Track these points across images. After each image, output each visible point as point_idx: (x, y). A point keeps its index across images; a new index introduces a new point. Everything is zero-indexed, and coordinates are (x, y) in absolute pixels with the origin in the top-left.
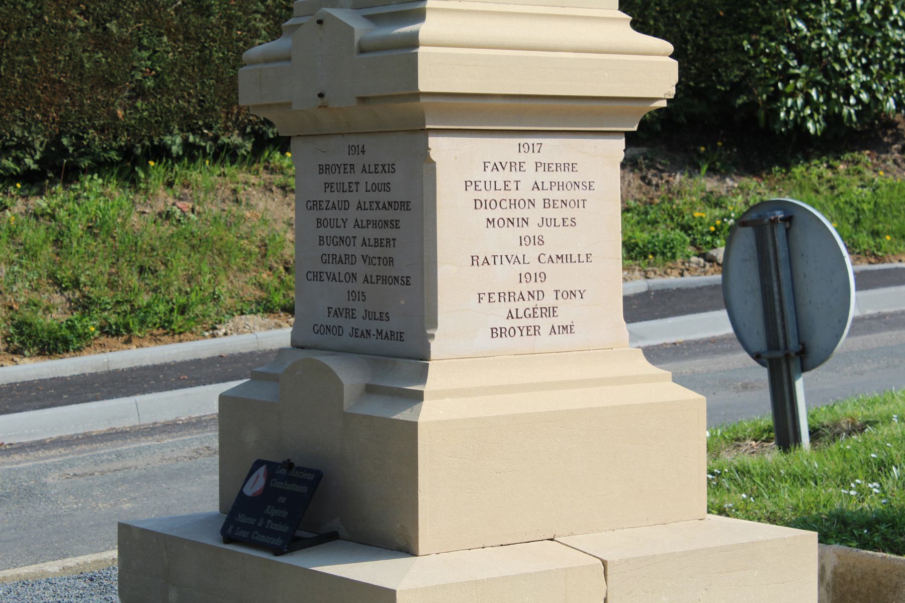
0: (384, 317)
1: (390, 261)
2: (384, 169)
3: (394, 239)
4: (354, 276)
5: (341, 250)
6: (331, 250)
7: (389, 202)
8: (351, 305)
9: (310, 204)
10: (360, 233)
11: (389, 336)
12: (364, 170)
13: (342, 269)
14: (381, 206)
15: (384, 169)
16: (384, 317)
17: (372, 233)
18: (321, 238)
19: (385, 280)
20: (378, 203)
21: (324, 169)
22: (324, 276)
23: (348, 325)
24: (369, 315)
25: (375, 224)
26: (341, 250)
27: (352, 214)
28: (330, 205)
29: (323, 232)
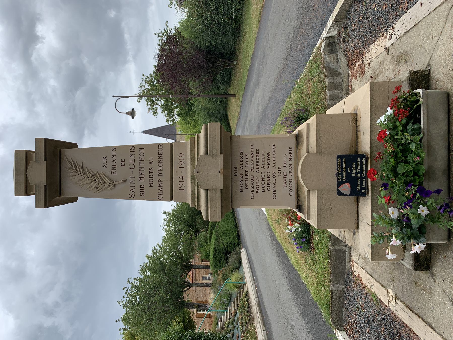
0: (285, 157)
1: (268, 154)
2: (241, 157)
5: (266, 179)
6: (266, 185)
10: (261, 170)
12: (241, 168)
13: (272, 179)
14: (252, 159)
15: (241, 157)
16: (285, 157)
17: (260, 164)
18: (263, 191)
19: (274, 157)
20: (252, 160)
21: (241, 191)
22: (274, 189)
23: (289, 177)
24: (285, 166)
26: (266, 179)
27: (255, 174)
28: (252, 186)
29: (260, 190)
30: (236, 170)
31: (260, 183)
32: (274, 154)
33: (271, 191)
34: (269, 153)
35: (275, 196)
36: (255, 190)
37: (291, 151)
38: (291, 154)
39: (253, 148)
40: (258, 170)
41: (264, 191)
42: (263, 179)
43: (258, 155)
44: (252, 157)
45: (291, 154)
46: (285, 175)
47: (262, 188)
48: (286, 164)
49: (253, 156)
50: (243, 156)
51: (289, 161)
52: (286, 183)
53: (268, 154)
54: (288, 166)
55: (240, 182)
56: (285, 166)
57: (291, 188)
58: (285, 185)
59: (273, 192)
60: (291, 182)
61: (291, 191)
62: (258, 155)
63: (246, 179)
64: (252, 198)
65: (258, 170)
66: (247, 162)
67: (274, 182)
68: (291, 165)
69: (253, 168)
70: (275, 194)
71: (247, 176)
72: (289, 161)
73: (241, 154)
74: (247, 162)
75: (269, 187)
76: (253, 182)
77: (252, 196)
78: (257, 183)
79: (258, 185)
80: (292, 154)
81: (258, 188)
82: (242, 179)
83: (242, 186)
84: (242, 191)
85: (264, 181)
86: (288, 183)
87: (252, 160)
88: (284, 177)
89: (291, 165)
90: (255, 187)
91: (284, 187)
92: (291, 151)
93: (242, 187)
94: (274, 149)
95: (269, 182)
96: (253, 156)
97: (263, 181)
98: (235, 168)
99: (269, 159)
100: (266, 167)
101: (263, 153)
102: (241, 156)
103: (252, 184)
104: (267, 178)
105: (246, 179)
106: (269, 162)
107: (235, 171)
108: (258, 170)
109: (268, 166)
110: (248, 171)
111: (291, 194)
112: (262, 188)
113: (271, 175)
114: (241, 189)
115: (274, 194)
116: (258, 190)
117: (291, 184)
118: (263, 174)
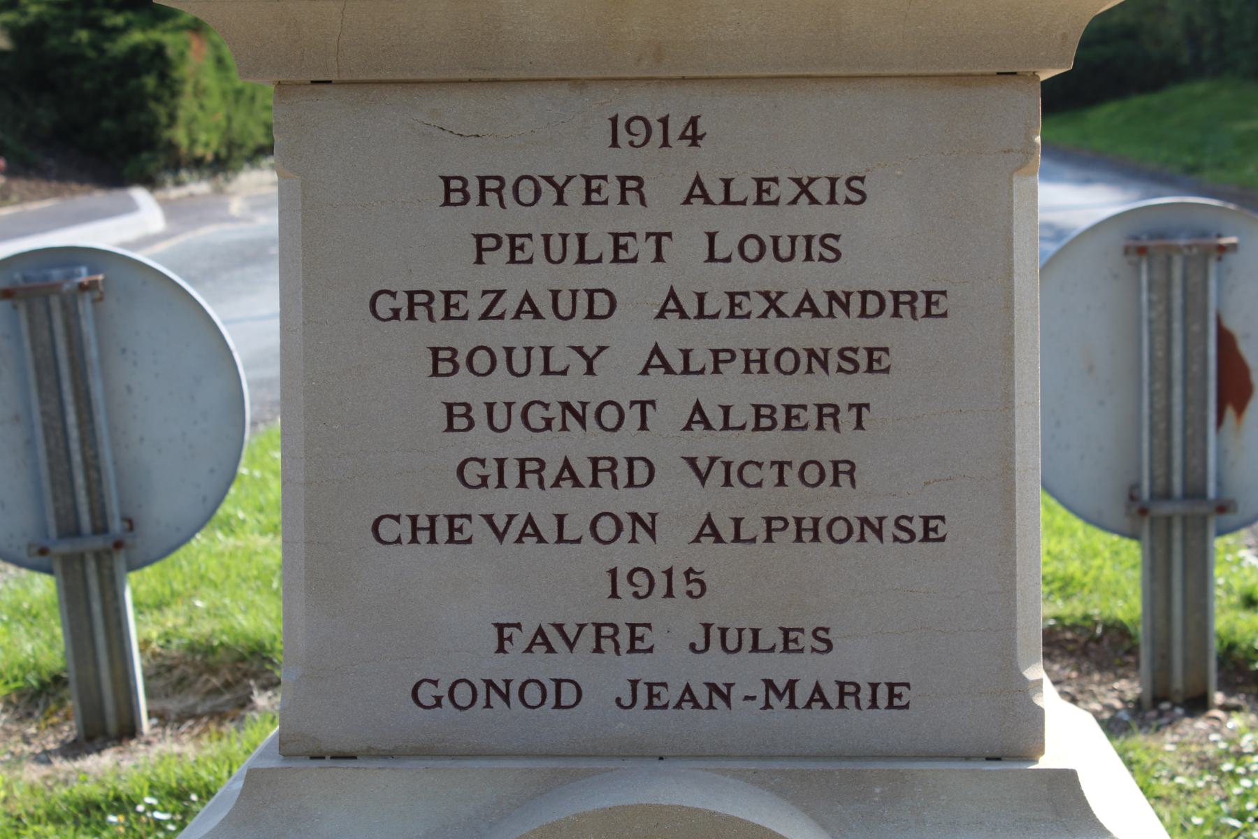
0: (806, 640)
1: (843, 471)
2: (804, 190)
3: (859, 408)
4: (646, 525)
7: (832, 296)
8: (626, 611)
9: (384, 306)
11: (833, 698)
12: (697, 192)
14: (788, 304)
15: (804, 190)
16: (806, 640)
20: (772, 302)
25: (757, 362)
28: (509, 303)
29: (462, 387)
30: (674, 134)
31: (537, 386)
32: (840, 530)
33: (456, 500)
34: (844, 479)
35: (407, 536)
36: (463, 336)
37: (865, 695)
38: (832, 695)
39: (904, 310)
40: (669, 370)
41: (460, 423)
42: (581, 420)
43: (824, 365)
44: (807, 305)
45: (832, 695)
46: (624, 638)
47: (490, 407)
48: (732, 643)
49: (816, 313)
50: (825, 210)
51: (769, 684)
52: (539, 650)
53: (843, 471)
54: (716, 666)
55: (549, 179)
56: (715, 634)
57: (494, 696)
58: (521, 639)
59: (451, 519)
60: (551, 699)
61: (463, 693)
62: (824, 365)
63: (582, 238)
64: (384, 306)
65: (677, 365)
66: (752, 248)
67: (548, 529)
68: (726, 699)
69: (691, 308)
70: (423, 536)
71: (609, 255)
72: (769, 684)
73: (842, 191)
74: (752, 248)
75: (493, 481)
76: (544, 305)
77: (402, 302)
78: (538, 356)
79: (520, 366)
80: (835, 714)
81: (482, 361)
82: (575, 192)
83: (508, 193)
84: (456, 197)
85: (557, 424)
86: (544, 667)
87: (772, 302)
88: (598, 627)
89: (726, 699)
90: (497, 335)
91: (500, 627)
92: (865, 695)
93: (491, 198)
94: (889, 528)
95: (550, 475)
96: (816, 313)
97: (555, 411)
98: (693, 122)
99: (791, 475)
100: (704, 444)
101: (847, 418)
102: (820, 190)
103: (527, 306)
104: (595, 461)
105: (582, 238)
106: (751, 474)
107: (664, 121)
108: (677, 365)
109: (719, 469)
110: (659, 258)
111: (426, 694)
112: (490, 407)
113: (624, 502)
114: (473, 188)
115: (423, 522)
116: (461, 359)
117: (533, 693)
118: (633, 415)
